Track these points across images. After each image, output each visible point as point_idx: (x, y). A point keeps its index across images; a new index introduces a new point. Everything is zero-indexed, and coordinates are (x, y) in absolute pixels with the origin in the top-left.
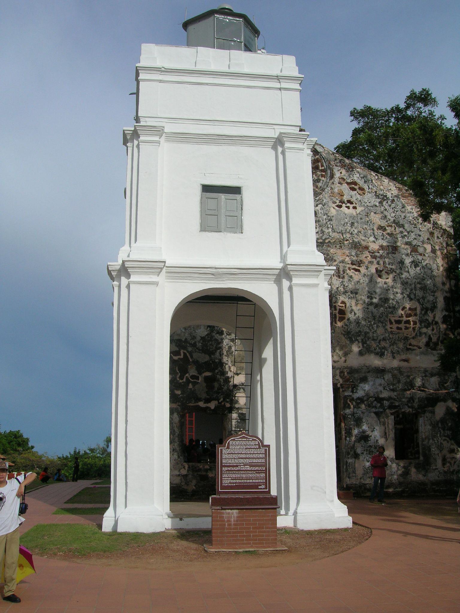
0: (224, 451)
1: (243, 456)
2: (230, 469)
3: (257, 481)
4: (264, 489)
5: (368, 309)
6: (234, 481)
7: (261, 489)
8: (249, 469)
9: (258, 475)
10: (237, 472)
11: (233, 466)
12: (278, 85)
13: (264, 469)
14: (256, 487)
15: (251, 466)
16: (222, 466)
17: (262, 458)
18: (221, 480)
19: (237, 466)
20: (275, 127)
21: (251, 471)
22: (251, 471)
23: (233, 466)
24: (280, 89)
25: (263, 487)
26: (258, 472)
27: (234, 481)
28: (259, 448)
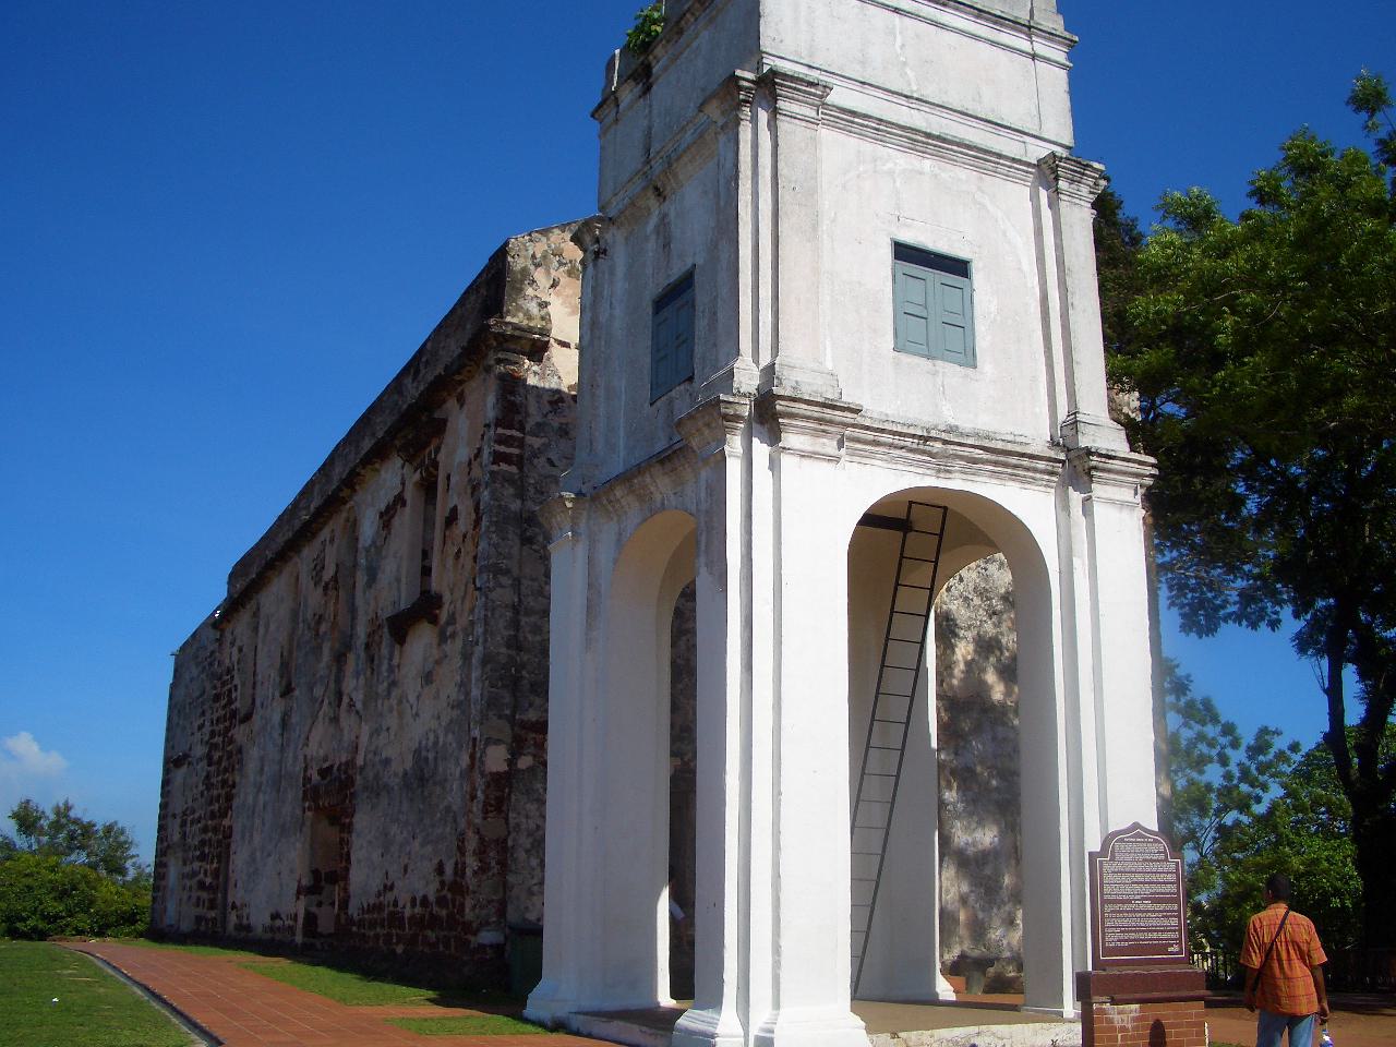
0: (1106, 866)
1: (1139, 878)
2: (1117, 907)
3: (1165, 936)
4: (1177, 953)
5: (986, 570)
6: (1127, 936)
7: (1172, 953)
8: (1150, 907)
9: (1166, 922)
10: (1130, 915)
11: (1123, 902)
12: (1024, 45)
13: (1176, 908)
14: (1163, 949)
15: (1155, 901)
16: (1104, 902)
17: (1171, 883)
18: (1103, 934)
19: (1129, 902)
20: (1026, 138)
21: (1154, 912)
22: (1154, 912)
23: (1123, 902)
24: (1034, 57)
25: (1175, 948)
26: (1167, 915)
27: (1127, 936)
28: (1166, 860)
